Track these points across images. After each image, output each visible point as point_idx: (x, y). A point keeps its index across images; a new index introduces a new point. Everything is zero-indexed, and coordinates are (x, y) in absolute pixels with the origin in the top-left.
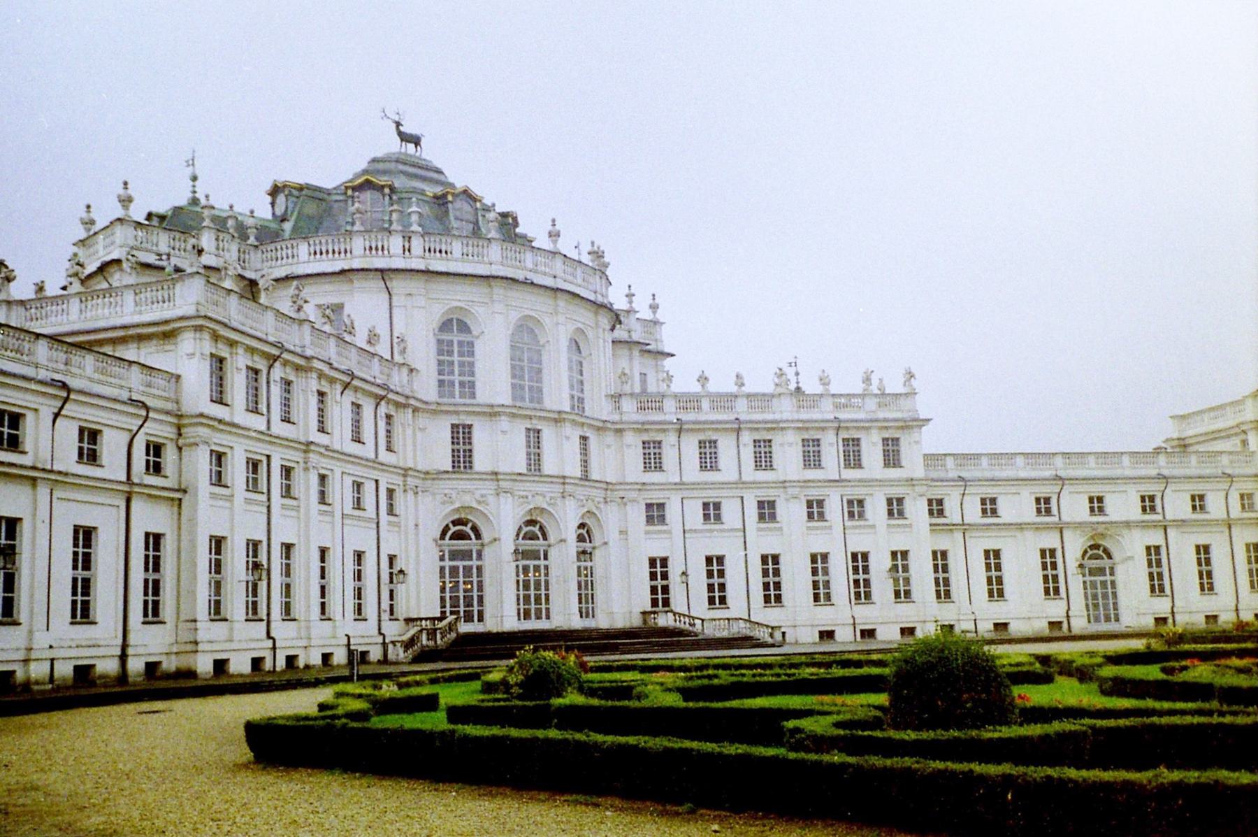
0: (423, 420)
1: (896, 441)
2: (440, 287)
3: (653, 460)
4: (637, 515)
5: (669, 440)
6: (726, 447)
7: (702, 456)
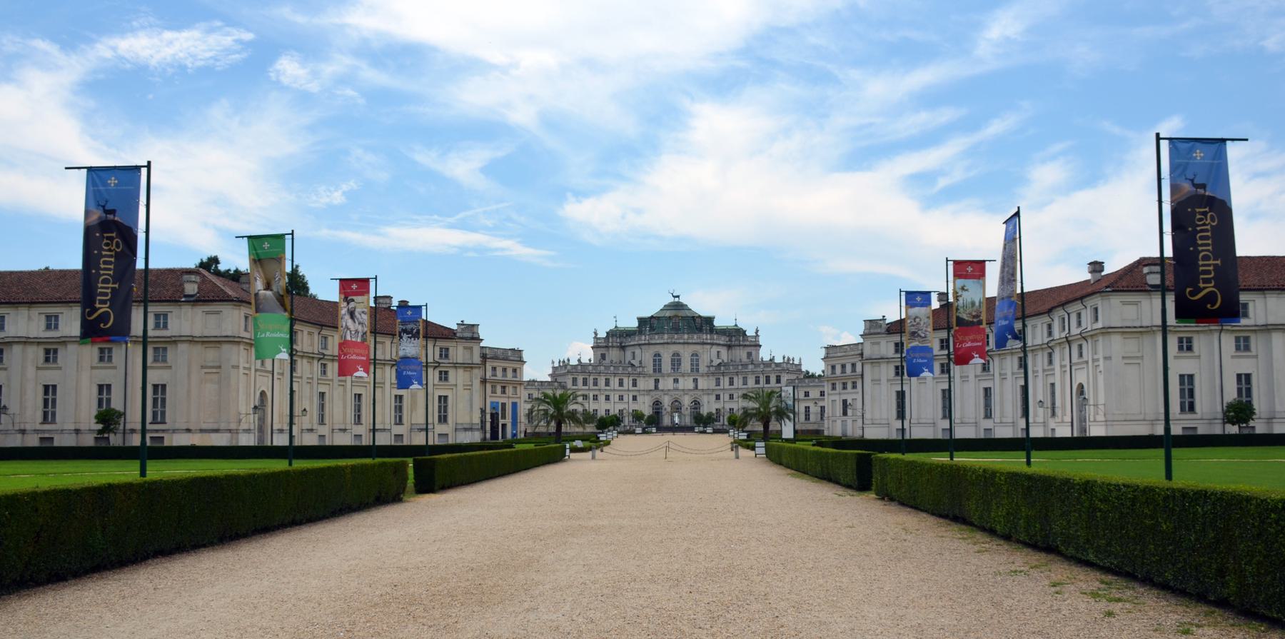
0: (647, 379)
1: (780, 376)
2: (651, 346)
3: (718, 384)
4: (714, 397)
5: (722, 377)
6: (735, 380)
7: (730, 382)
